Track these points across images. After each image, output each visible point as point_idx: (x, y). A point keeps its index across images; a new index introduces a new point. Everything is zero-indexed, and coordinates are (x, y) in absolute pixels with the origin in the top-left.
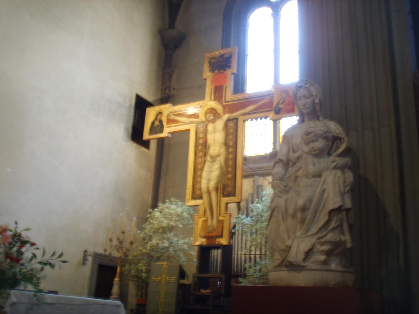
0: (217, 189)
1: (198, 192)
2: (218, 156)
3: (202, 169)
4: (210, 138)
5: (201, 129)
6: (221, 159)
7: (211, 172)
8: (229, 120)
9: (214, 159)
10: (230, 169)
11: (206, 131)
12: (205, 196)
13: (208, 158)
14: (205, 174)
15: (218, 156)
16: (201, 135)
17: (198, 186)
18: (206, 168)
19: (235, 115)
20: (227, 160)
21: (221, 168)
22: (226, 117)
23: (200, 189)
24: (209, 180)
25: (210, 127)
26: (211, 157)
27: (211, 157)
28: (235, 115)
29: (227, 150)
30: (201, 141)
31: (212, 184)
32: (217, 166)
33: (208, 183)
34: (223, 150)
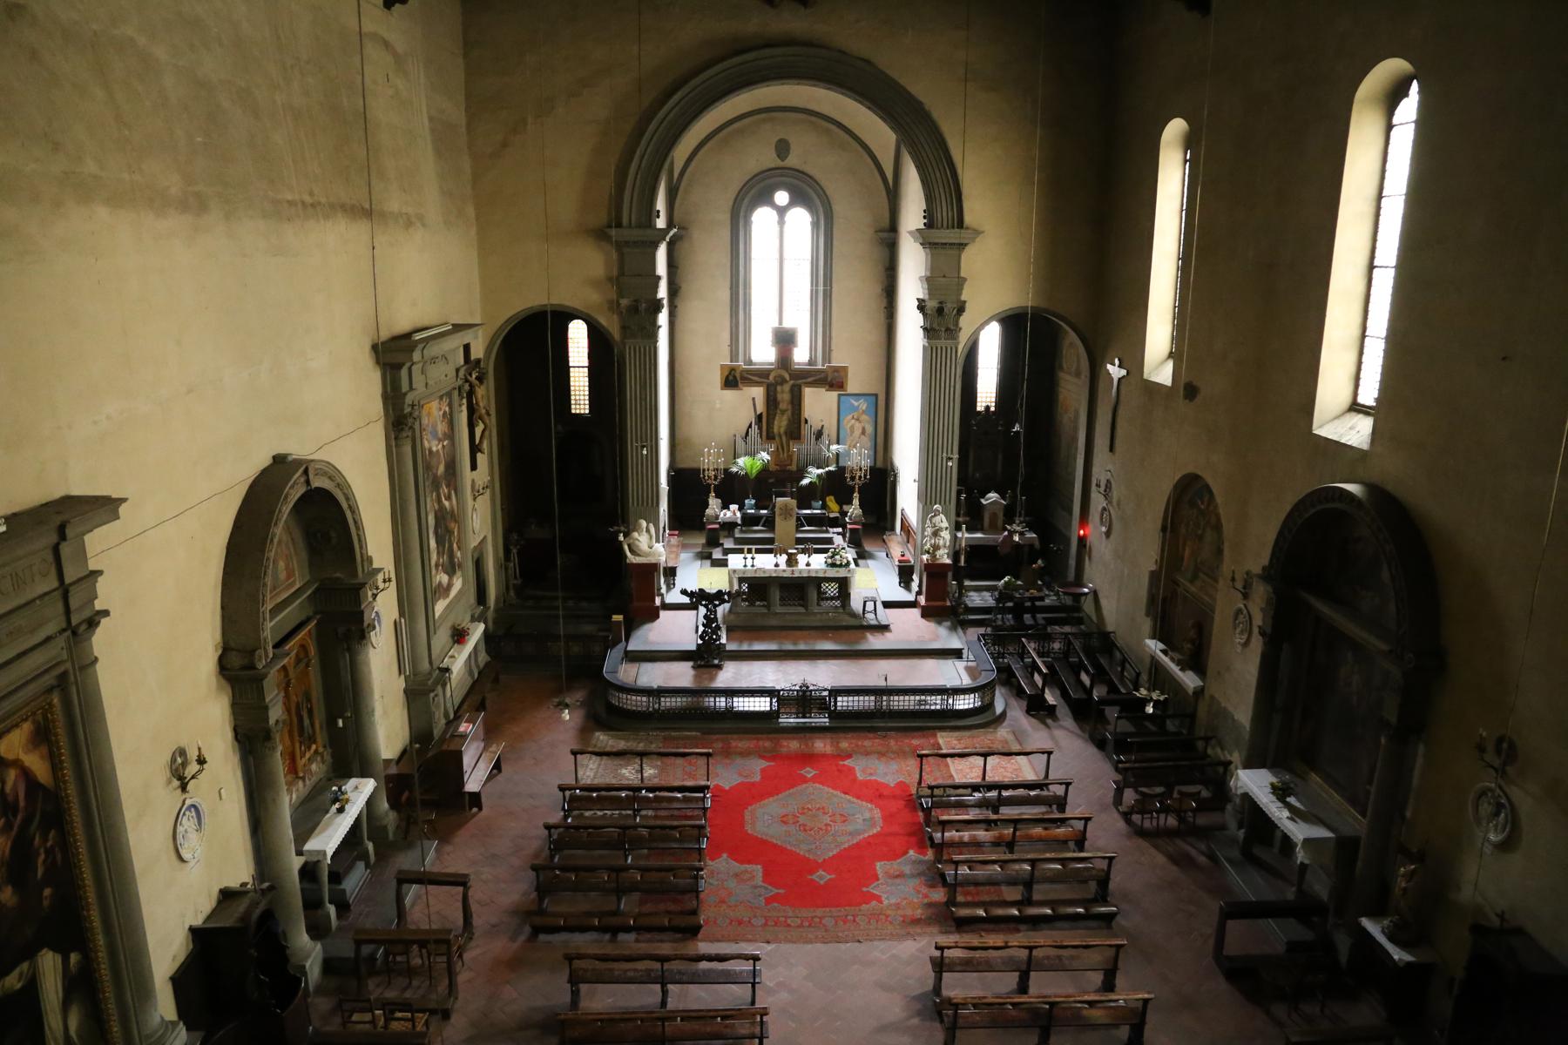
0: (786, 433)
1: (771, 435)
3: (774, 419)
4: (779, 397)
6: (789, 412)
7: (781, 422)
8: (793, 386)
9: (783, 412)
12: (777, 438)
13: (778, 411)
14: (776, 422)
16: (772, 393)
17: (771, 430)
18: (777, 418)
20: (793, 414)
22: (792, 382)
23: (773, 432)
24: (780, 427)
25: (779, 388)
26: (781, 411)
27: (781, 411)
29: (793, 407)
30: (772, 398)
31: (782, 430)
32: (785, 417)
34: (790, 407)
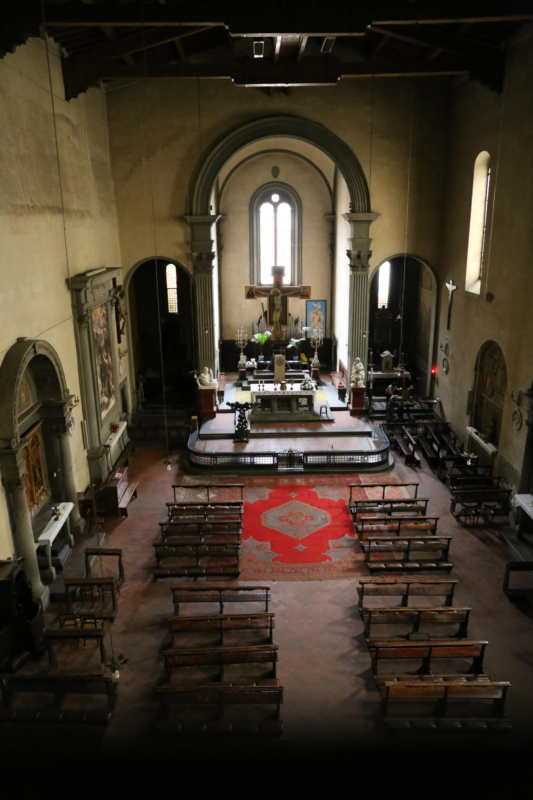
0: (279, 321)
2: (280, 309)
4: (276, 302)
5: (272, 298)
6: (281, 310)
10: (284, 315)
11: (273, 299)
12: (275, 324)
13: (275, 310)
14: (274, 316)
15: (280, 309)
18: (274, 313)
19: (285, 294)
21: (281, 314)
22: (282, 295)
23: (273, 321)
24: (276, 318)
25: (275, 298)
28: (285, 294)
29: (283, 308)
31: (277, 320)
32: (279, 313)
33: (276, 319)
34: (281, 307)
